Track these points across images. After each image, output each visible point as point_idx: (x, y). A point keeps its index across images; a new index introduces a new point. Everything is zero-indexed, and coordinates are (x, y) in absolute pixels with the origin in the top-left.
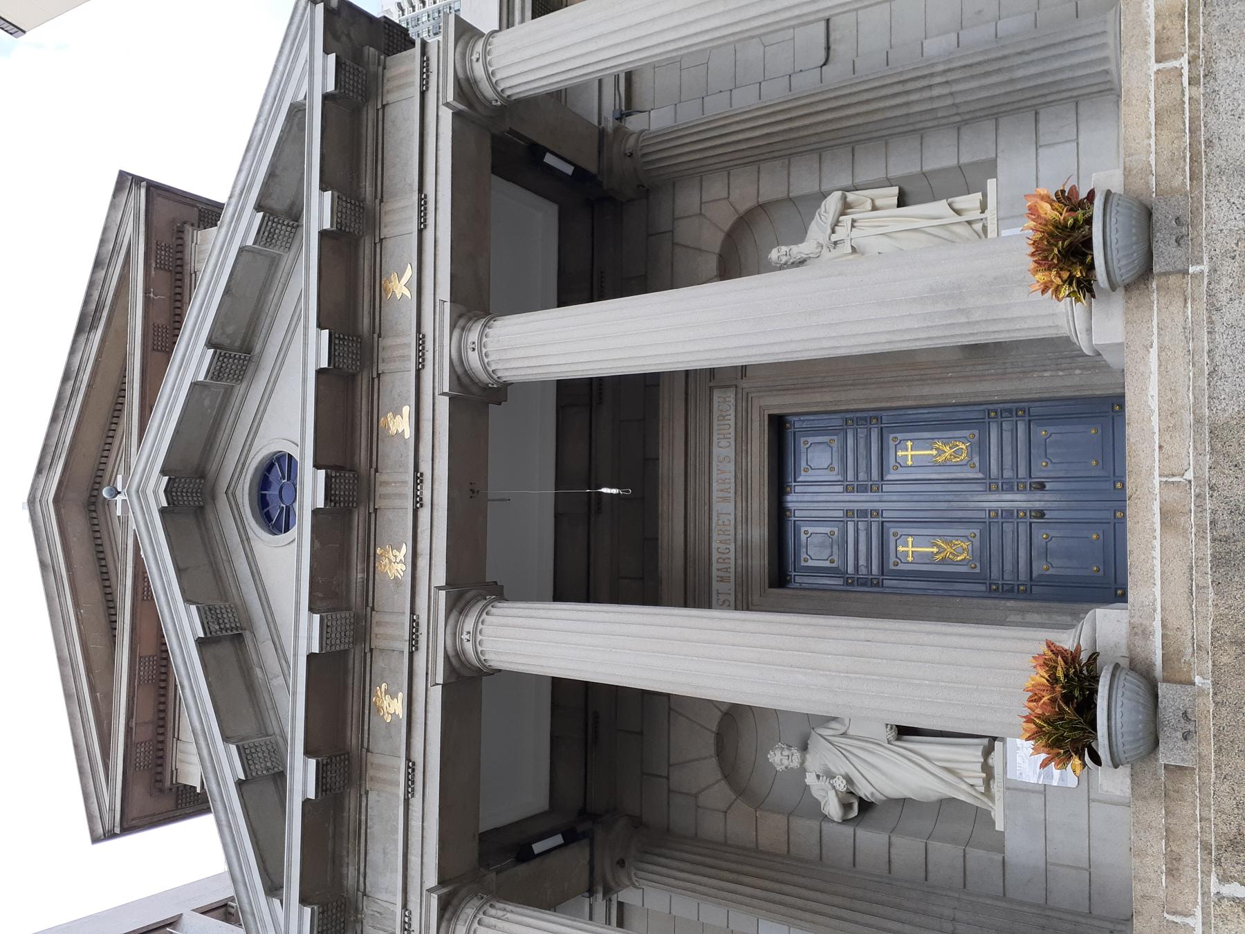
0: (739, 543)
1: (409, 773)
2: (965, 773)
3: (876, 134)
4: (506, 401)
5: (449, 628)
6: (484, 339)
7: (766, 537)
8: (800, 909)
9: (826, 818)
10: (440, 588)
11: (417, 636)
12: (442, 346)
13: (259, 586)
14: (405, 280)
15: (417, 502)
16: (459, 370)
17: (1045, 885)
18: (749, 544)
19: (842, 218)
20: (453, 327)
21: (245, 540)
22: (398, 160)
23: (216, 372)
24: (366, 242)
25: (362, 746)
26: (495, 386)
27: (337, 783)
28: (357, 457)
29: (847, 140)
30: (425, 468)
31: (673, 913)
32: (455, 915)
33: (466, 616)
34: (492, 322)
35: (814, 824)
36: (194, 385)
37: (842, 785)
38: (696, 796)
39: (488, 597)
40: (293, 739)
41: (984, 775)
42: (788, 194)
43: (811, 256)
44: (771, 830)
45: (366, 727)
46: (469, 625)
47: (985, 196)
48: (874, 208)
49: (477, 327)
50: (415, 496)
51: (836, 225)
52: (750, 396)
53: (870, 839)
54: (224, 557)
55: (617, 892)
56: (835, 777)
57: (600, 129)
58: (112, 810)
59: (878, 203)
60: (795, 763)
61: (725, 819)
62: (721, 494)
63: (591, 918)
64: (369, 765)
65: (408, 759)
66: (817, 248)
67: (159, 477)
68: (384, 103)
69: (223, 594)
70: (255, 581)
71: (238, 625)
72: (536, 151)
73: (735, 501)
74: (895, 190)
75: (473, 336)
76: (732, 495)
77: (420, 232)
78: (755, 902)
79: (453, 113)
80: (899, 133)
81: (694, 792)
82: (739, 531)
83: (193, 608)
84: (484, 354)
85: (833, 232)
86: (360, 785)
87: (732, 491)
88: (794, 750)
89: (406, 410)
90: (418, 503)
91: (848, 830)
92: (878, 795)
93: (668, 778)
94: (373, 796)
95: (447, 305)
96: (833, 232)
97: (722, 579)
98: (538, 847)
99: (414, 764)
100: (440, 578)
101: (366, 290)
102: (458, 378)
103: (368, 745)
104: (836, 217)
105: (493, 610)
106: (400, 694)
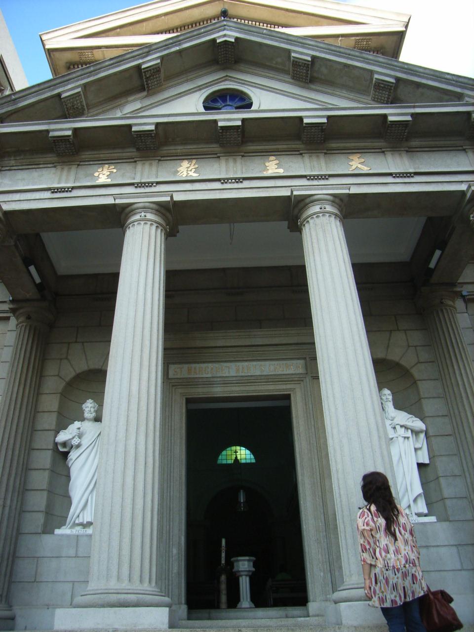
0: (212, 380)
1: (65, 189)
2: (85, 512)
3: (461, 448)
4: (291, 231)
5: (148, 204)
6: (328, 215)
7: (215, 396)
8: (6, 420)
9: (57, 432)
10: (172, 197)
11: (143, 187)
12: (322, 189)
13: (173, 98)
14: (360, 166)
15: (224, 180)
16: (308, 200)
17: (26, 556)
18: (211, 386)
19: (410, 431)
20: (334, 195)
21: (199, 88)
22: (433, 159)
23: (297, 63)
24: (382, 143)
25: (81, 162)
26: (299, 223)
27: (59, 149)
28: (250, 144)
29: (456, 431)
30: (246, 184)
31: (5, 348)
33: (156, 214)
34: (339, 219)
35: (53, 427)
36: (289, 52)
37: (75, 442)
38: (67, 358)
39: (168, 227)
41: (85, 523)
42: (422, 398)
43: (387, 414)
44: (50, 402)
45: (91, 163)
46: (150, 216)
47: (426, 515)
48: (416, 450)
49: (336, 211)
50: (228, 179)
51: (405, 427)
52: (302, 382)
53: (44, 459)
54: (189, 78)
55: (14, 316)
56: (80, 438)
57: (456, 283)
59: (419, 452)
60: (86, 415)
61: (55, 376)
62: (241, 367)
64: (70, 166)
65: (73, 188)
66: (392, 417)
67: (233, 36)
68: (467, 150)
69: (169, 78)
70: (176, 95)
71: (150, 88)
72: (442, 246)
73: (236, 376)
74: (427, 461)
75: (329, 208)
76: (241, 374)
77: (390, 174)
78: (10, 394)
79: (464, 191)
80: (462, 463)
81: (69, 357)
82: (219, 380)
83: (159, 61)
84: (319, 215)
85: (402, 426)
86: (59, 163)
87: (243, 374)
88: (94, 414)
92: (71, 462)
93: (76, 342)
94: (53, 170)
95: (347, 191)
96: (402, 426)
97: (189, 371)
98: (32, 269)
99: (70, 191)
100: (177, 197)
101: (353, 144)
102: (303, 200)
103: (81, 165)
104: (410, 427)
105: (159, 231)
106: (109, 180)
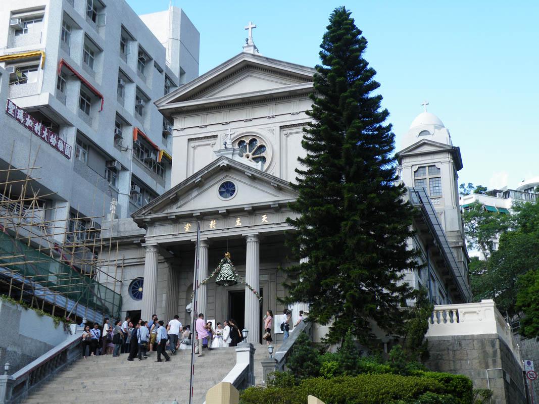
21: (218, 182)
30: (230, 230)
32: (155, 248)
40: (200, 101)
58: (163, 106)
63: (159, 263)
89: (240, 224)
90: (223, 230)
91: (184, 311)
94: (171, 226)
98: (170, 252)
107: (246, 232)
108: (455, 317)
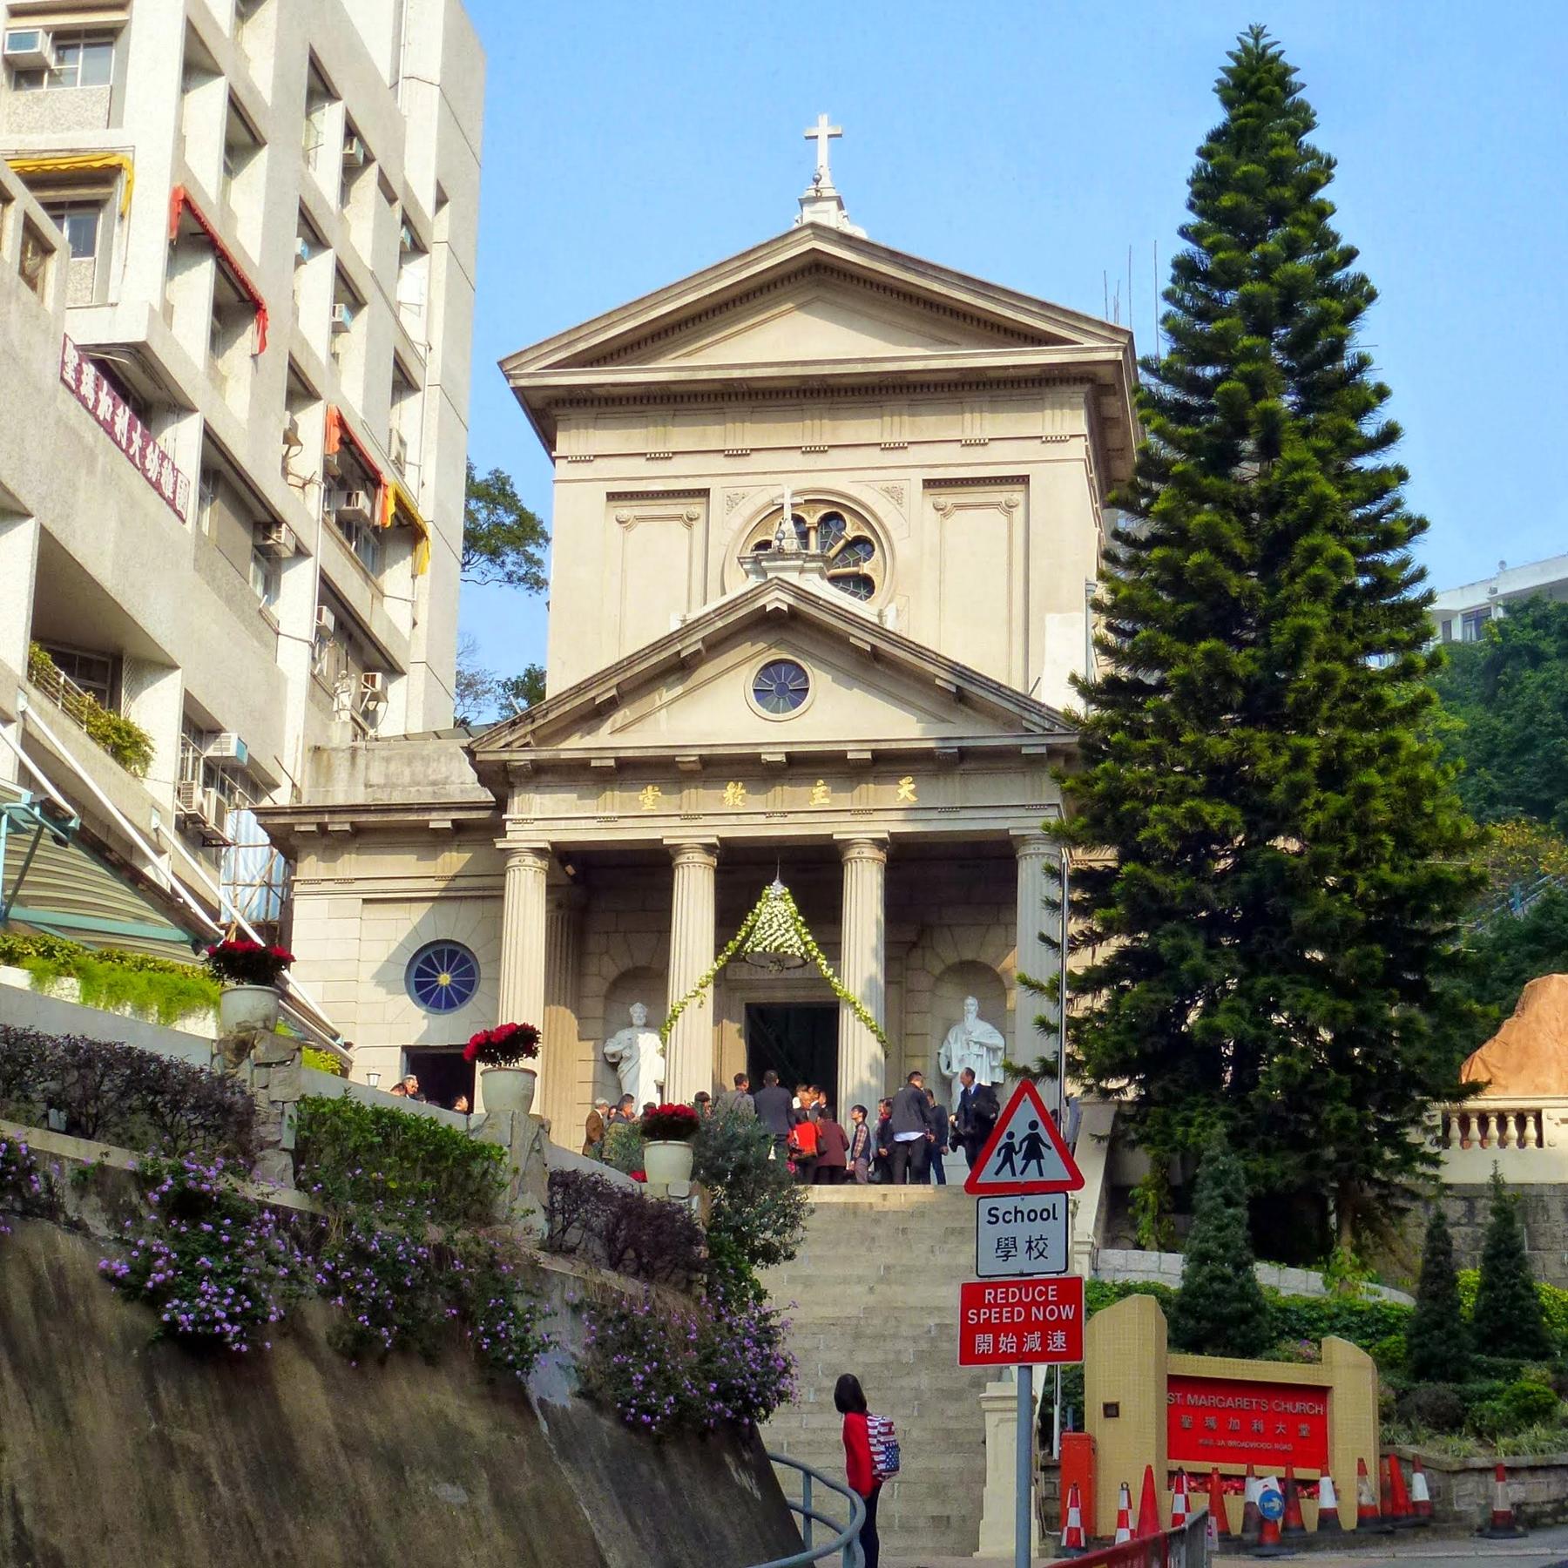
58: (529, 375)
89: (827, 801)
107: (844, 828)
108: (1531, 1131)
